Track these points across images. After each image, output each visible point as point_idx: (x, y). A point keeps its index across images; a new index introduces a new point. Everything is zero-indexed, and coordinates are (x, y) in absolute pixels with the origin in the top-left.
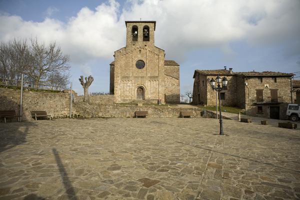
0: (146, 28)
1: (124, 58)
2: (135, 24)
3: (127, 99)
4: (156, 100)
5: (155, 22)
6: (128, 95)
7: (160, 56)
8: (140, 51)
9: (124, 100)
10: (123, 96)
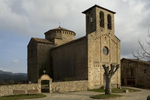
0: (109, 17)
1: (95, 43)
2: (102, 10)
3: (98, 84)
4: (115, 84)
5: (114, 13)
6: (98, 80)
7: (118, 45)
8: (106, 38)
9: (96, 86)
10: (94, 82)
